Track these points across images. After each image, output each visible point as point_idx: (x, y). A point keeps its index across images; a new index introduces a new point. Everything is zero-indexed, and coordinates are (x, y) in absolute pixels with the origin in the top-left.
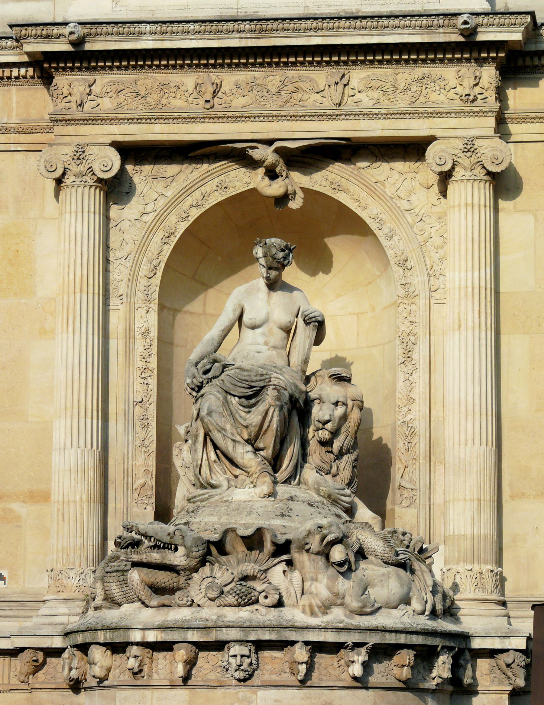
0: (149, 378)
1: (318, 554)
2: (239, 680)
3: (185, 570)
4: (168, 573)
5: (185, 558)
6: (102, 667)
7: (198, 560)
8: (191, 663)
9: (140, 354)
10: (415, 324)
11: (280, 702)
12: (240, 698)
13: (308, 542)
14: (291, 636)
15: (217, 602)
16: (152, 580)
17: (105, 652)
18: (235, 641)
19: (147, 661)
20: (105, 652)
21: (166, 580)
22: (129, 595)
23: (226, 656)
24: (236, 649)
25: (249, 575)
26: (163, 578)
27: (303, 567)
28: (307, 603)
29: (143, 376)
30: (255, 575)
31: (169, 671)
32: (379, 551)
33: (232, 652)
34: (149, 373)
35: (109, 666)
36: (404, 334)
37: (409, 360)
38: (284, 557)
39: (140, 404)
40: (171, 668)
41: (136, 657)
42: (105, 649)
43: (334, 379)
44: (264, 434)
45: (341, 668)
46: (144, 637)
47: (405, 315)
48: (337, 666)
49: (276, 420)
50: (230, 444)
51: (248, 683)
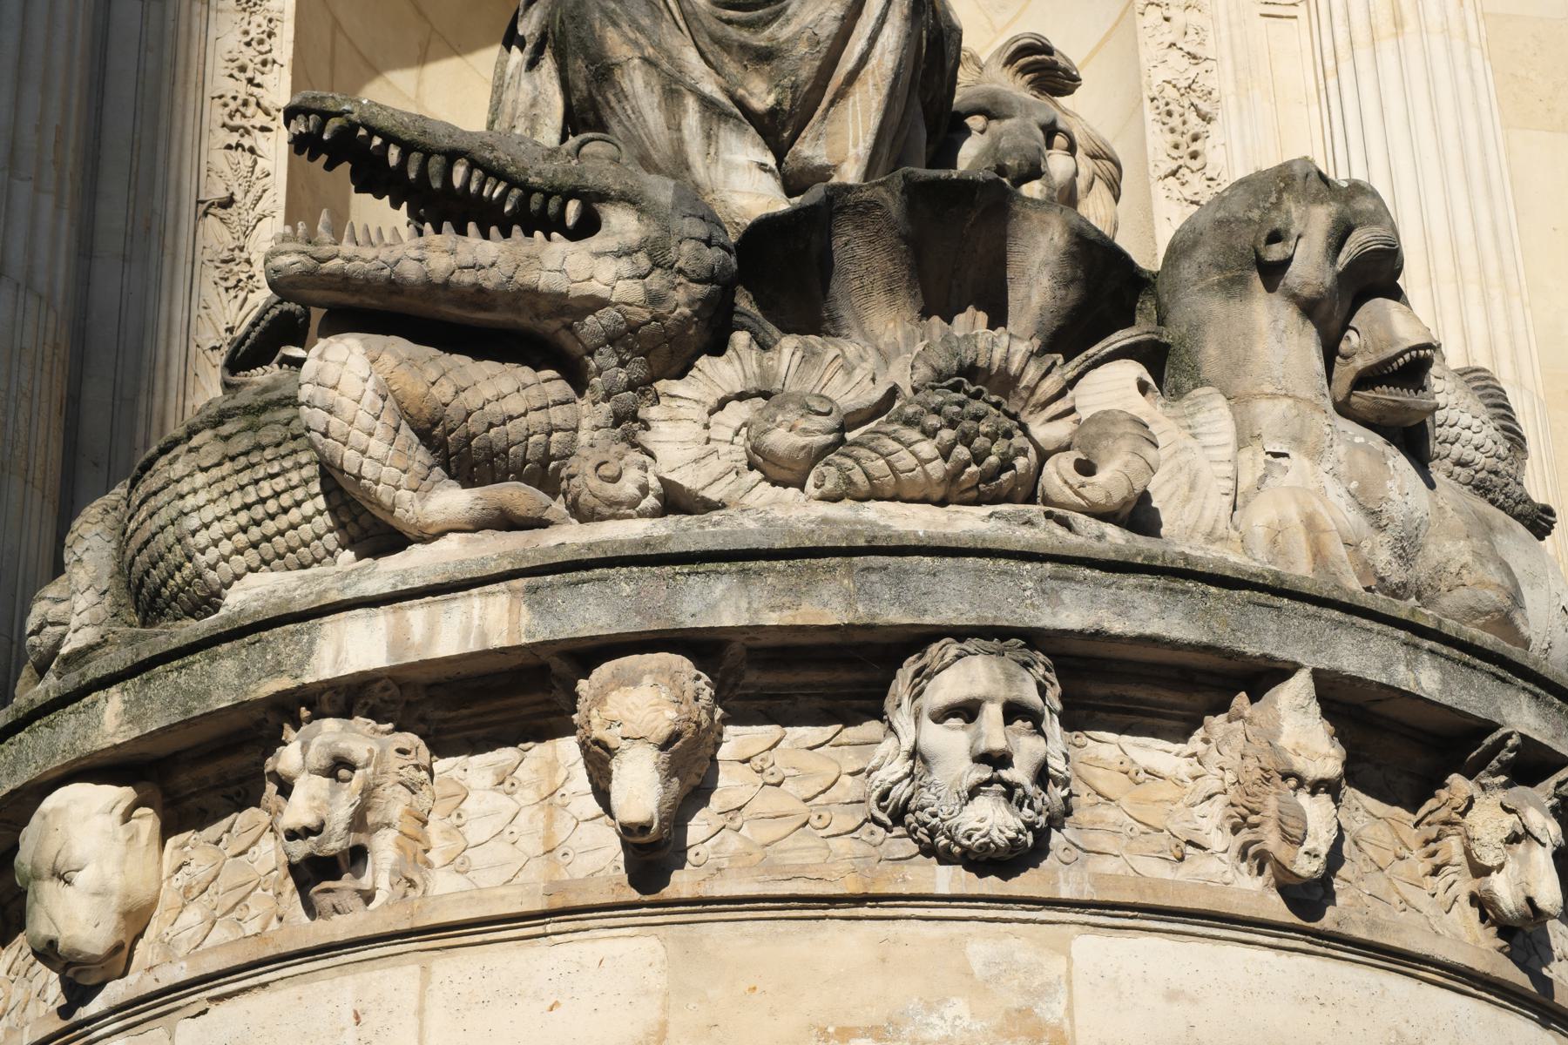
0: (256, 133)
1: (1309, 308)
2: (985, 860)
3: (623, 338)
4: (526, 373)
5: (643, 261)
6: (101, 893)
7: (699, 290)
8: (691, 768)
9: (228, 56)
10: (1207, 65)
11: (1193, 1001)
12: (977, 967)
13: (1278, 224)
14: (1259, 634)
15: (827, 474)
16: (444, 392)
17: (127, 817)
18: (960, 634)
19: (394, 804)
20: (127, 817)
21: (514, 405)
22: (283, 521)
23: (902, 719)
24: (967, 675)
25: (982, 363)
26: (498, 392)
27: (1238, 365)
28: (1293, 514)
29: (238, 121)
30: (1014, 368)
31: (532, 845)
32: (1477, 439)
33: (949, 686)
34: (261, 119)
35: (142, 894)
36: (1171, 93)
37: (1195, 164)
38: (1120, 338)
39: (220, 212)
40: (549, 827)
41: (338, 767)
42: (122, 795)
43: (1024, 70)
44: (841, 95)
45: (1439, 883)
46: (398, 641)
47: (1170, 39)
48: (1428, 865)
49: (891, 37)
50: (692, 117)
51: (1021, 885)
